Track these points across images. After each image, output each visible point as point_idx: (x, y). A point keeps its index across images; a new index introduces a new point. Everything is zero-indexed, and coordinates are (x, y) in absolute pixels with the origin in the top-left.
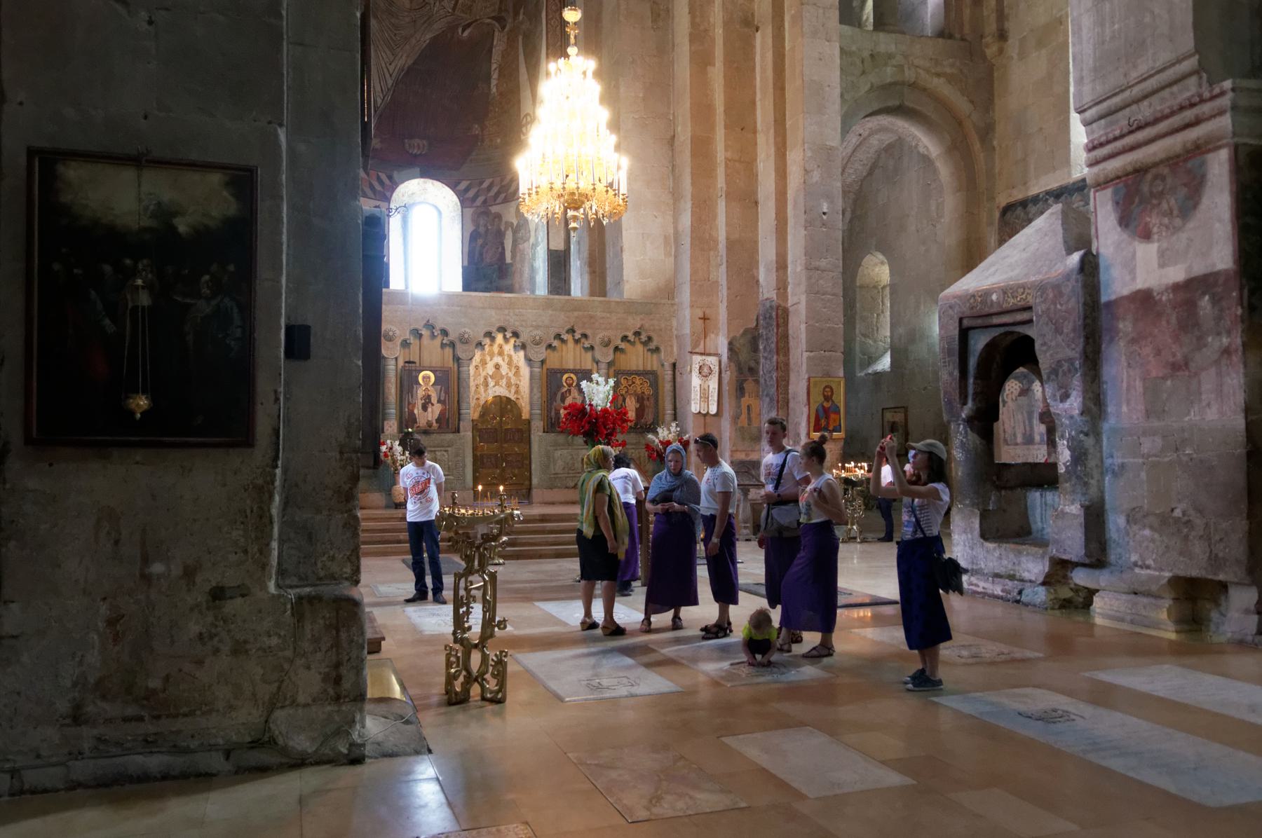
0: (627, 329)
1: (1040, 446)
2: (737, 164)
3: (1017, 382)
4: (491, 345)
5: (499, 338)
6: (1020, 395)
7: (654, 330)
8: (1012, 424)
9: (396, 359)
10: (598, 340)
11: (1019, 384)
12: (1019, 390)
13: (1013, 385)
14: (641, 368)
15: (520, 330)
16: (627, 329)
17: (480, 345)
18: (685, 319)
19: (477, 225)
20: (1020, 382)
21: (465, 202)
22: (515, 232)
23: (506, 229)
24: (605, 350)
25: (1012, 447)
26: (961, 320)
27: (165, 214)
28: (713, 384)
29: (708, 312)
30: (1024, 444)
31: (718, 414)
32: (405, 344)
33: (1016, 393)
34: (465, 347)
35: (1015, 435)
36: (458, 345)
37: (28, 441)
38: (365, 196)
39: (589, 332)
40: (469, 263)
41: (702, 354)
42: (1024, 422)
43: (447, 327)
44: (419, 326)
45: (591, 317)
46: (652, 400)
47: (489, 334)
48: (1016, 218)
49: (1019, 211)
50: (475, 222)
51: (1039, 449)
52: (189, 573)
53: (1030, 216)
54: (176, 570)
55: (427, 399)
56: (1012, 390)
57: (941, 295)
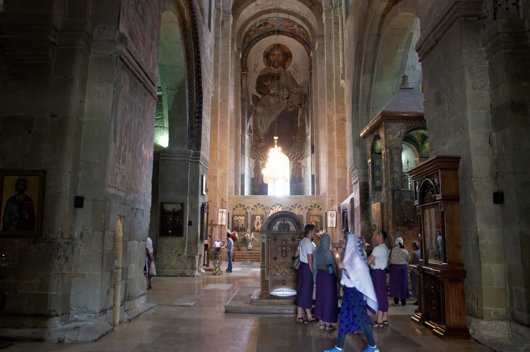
0: (312, 204)
2: (341, 158)
4: (275, 209)
5: (278, 207)
7: (320, 204)
9: (251, 213)
10: (304, 207)
14: (317, 214)
15: (282, 205)
16: (312, 204)
17: (271, 209)
18: (327, 202)
19: (294, 166)
21: (291, 159)
22: (305, 168)
23: (302, 167)
24: (305, 209)
26: (343, 210)
27: (174, 209)
28: (334, 219)
29: (333, 199)
31: (336, 227)
32: (253, 209)
34: (268, 209)
36: (266, 209)
37: (160, 236)
38: (261, 160)
39: (301, 205)
40: (292, 178)
41: (331, 211)
43: (263, 204)
44: (256, 204)
45: (302, 201)
46: (320, 223)
47: (274, 206)
50: (293, 165)
52: (176, 252)
54: (175, 251)
55: (258, 223)
57: (342, 204)
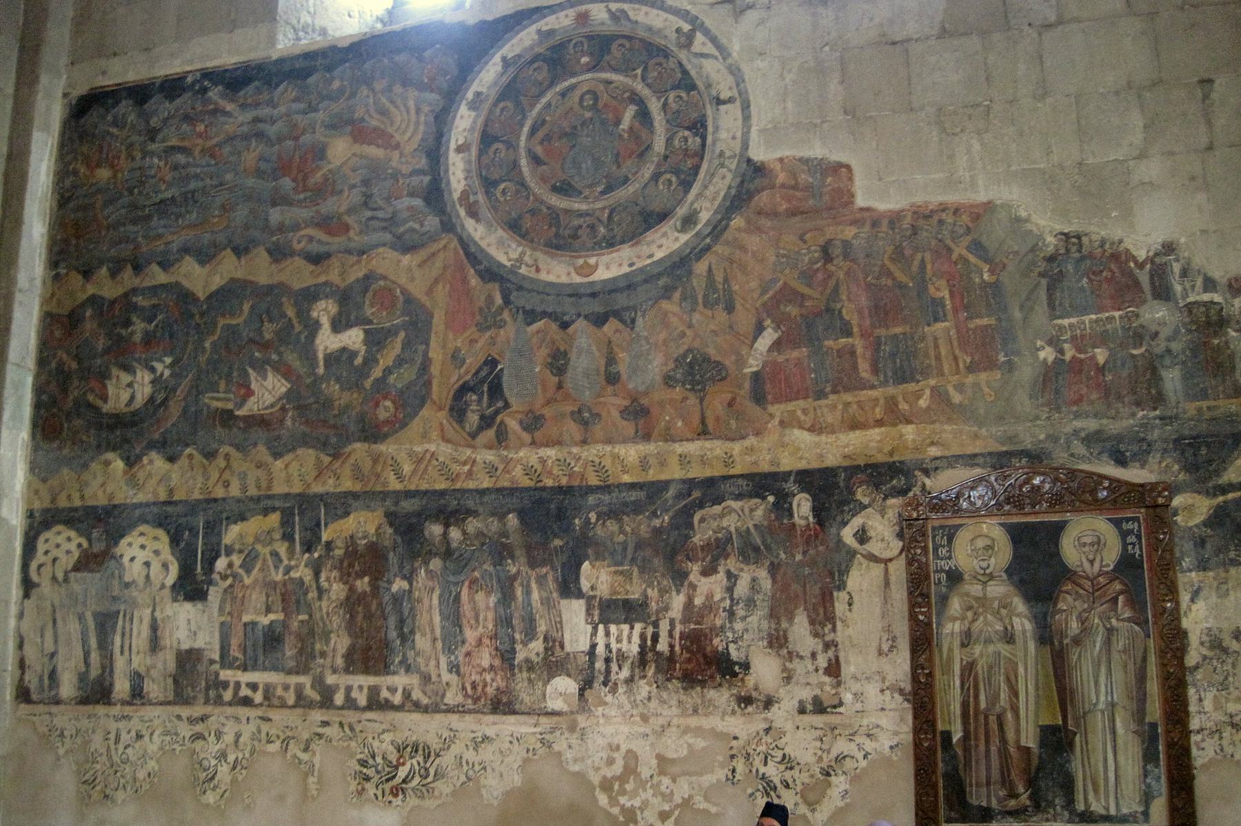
1: (128, 710)
3: (73, 534)
6: (77, 568)
8: (49, 646)
11: (77, 539)
12: (76, 554)
13: (59, 539)
20: (80, 533)
25: (41, 708)
30: (84, 701)
33: (67, 562)
35: (53, 675)
42: (85, 642)
48: (115, 123)
49: (125, 108)
51: (127, 718)
53: (154, 122)
56: (55, 553)
